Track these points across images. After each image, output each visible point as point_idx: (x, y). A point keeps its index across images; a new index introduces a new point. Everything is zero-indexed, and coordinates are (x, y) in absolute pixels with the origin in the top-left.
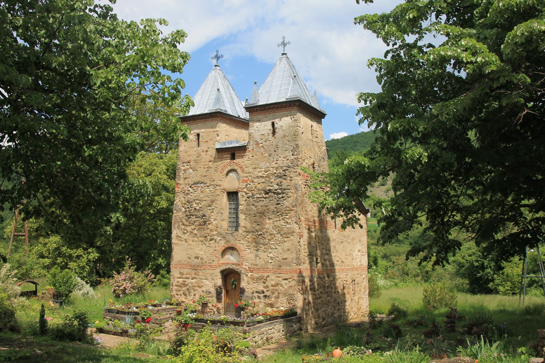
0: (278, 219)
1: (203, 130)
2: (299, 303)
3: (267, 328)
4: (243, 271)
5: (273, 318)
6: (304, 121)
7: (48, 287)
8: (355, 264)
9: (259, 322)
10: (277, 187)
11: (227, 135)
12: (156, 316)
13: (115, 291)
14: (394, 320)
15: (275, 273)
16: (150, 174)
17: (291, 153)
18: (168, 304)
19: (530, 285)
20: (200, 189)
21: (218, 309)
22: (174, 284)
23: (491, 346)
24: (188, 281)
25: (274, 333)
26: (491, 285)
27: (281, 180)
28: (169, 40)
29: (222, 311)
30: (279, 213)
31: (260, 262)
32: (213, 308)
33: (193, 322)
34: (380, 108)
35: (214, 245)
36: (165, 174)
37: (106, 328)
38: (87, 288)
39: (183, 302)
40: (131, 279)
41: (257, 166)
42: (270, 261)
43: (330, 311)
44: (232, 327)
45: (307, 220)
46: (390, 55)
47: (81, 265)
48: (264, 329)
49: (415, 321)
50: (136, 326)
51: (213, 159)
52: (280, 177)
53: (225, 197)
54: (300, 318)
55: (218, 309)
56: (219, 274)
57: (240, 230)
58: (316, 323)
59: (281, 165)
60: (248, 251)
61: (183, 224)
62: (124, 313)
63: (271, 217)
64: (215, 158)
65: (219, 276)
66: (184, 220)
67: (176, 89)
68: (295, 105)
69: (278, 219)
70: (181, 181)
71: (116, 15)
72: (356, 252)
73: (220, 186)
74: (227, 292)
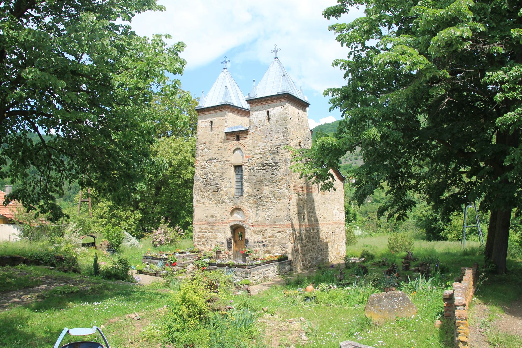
0: (273, 186)
1: (215, 118)
2: (289, 251)
3: (264, 270)
4: (247, 227)
5: (268, 262)
6: (292, 109)
7: (104, 240)
8: (334, 219)
9: (257, 265)
10: (271, 161)
11: (233, 122)
12: (181, 261)
13: (153, 242)
14: (364, 262)
15: (271, 227)
16: (178, 154)
17: (282, 135)
18: (191, 252)
19: (470, 233)
20: (213, 163)
21: (229, 255)
22: (196, 237)
23: (427, 281)
24: (207, 234)
25: (269, 273)
26: (442, 233)
27: (274, 155)
28: (172, 50)
29: (232, 257)
30: (273, 181)
31: (260, 219)
32: (225, 254)
33: (208, 265)
34: (346, 98)
35: (224, 207)
36: (190, 153)
37: (145, 270)
38: (134, 240)
39: (203, 250)
40: (165, 233)
41: (256, 145)
42: (267, 218)
43: (314, 256)
44: (236, 269)
45: (295, 186)
46: (352, 56)
47: (130, 223)
48: (261, 270)
49: (380, 263)
50: (166, 269)
51: (223, 141)
52: (274, 153)
54: (291, 261)
55: (229, 255)
56: (229, 229)
57: (244, 195)
58: (304, 265)
59: (275, 144)
60: (251, 211)
61: (202, 191)
62: (157, 259)
63: (267, 184)
64: (224, 140)
65: (229, 230)
66: (202, 188)
67: (174, 87)
68: (284, 97)
69: (273, 186)
70: (199, 158)
71: (134, 32)
72: (336, 210)
73: (228, 161)
74: (236, 242)
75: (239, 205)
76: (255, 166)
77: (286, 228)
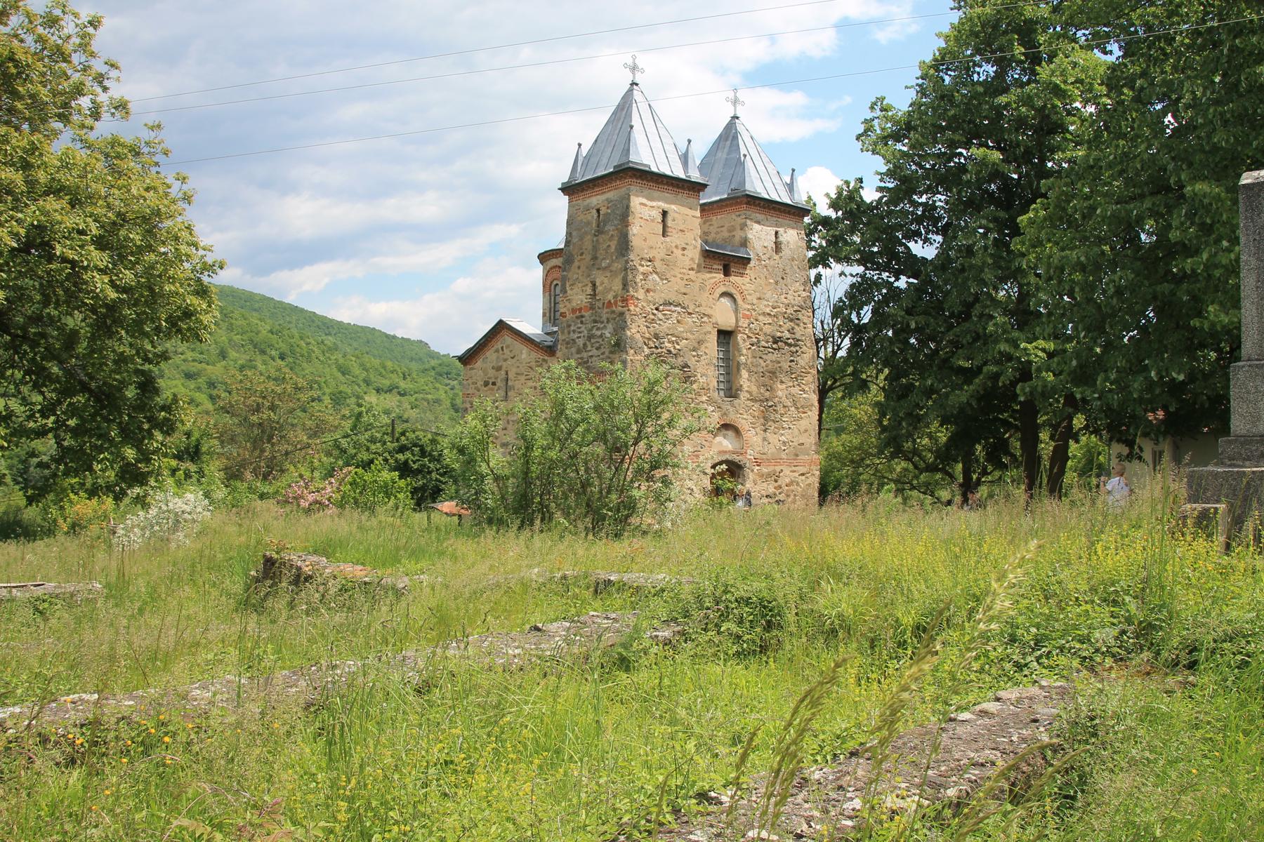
1: (673, 207)
10: (787, 335)
20: (675, 315)
31: (771, 450)
52: (791, 320)
53: (714, 337)
64: (699, 265)
75: (732, 418)
76: (761, 338)
77: (813, 467)
